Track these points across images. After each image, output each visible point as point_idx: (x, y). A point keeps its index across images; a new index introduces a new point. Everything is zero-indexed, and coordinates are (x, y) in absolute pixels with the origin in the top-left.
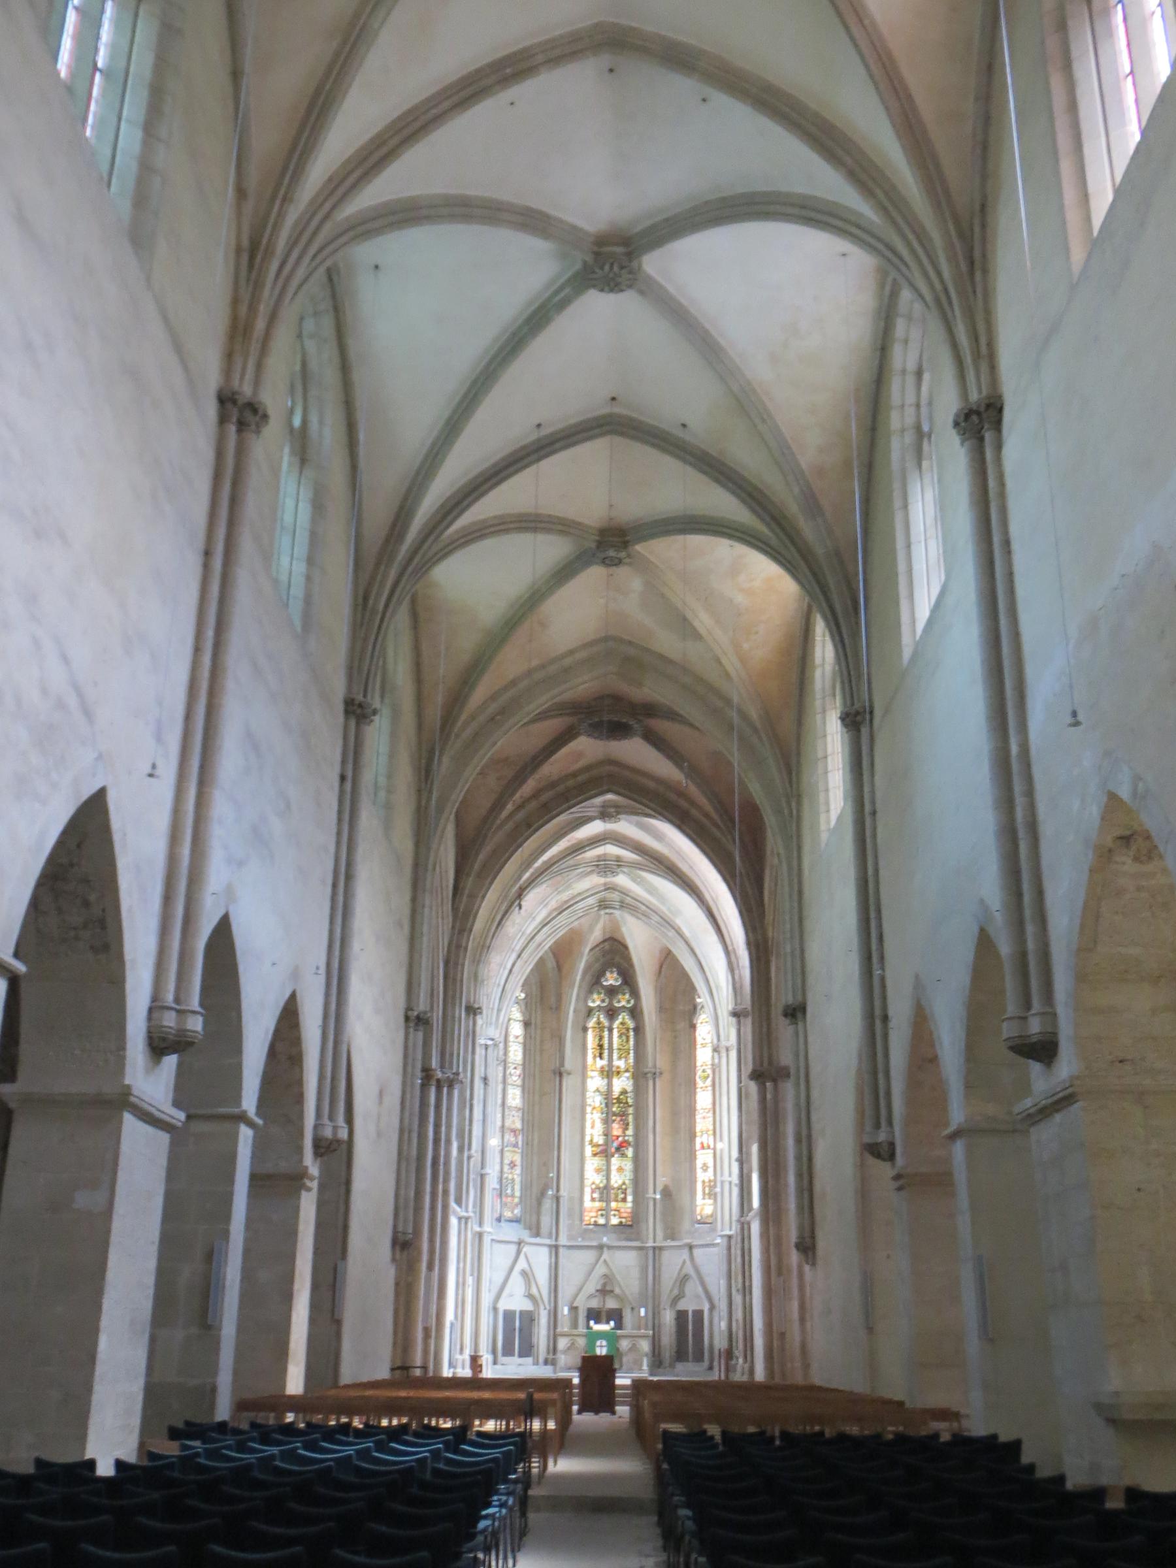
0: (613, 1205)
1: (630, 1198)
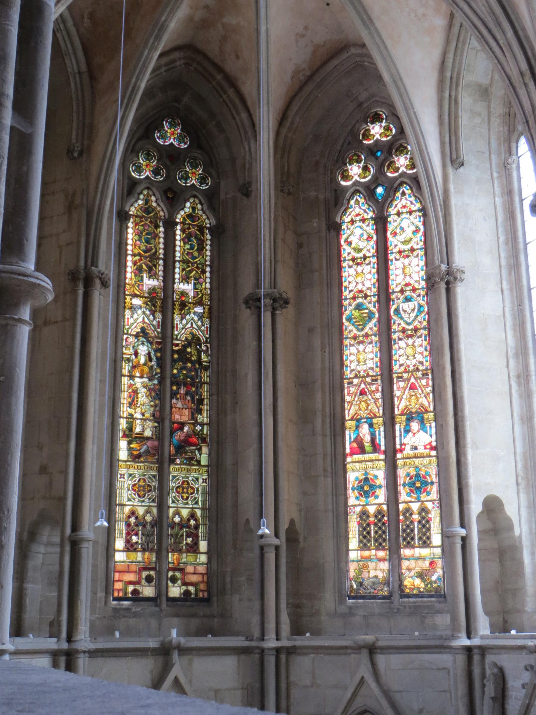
0: (172, 557)
1: (203, 545)
